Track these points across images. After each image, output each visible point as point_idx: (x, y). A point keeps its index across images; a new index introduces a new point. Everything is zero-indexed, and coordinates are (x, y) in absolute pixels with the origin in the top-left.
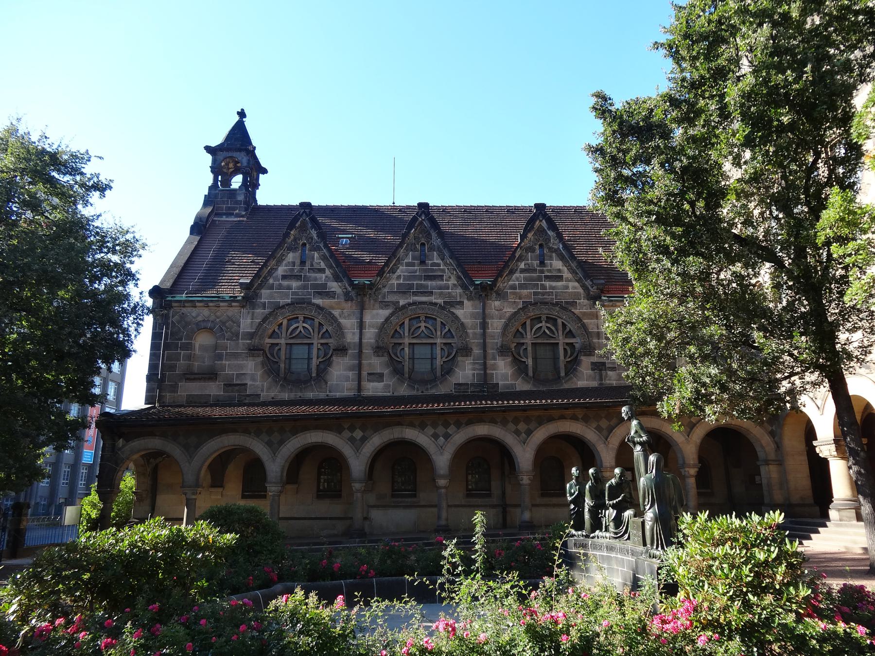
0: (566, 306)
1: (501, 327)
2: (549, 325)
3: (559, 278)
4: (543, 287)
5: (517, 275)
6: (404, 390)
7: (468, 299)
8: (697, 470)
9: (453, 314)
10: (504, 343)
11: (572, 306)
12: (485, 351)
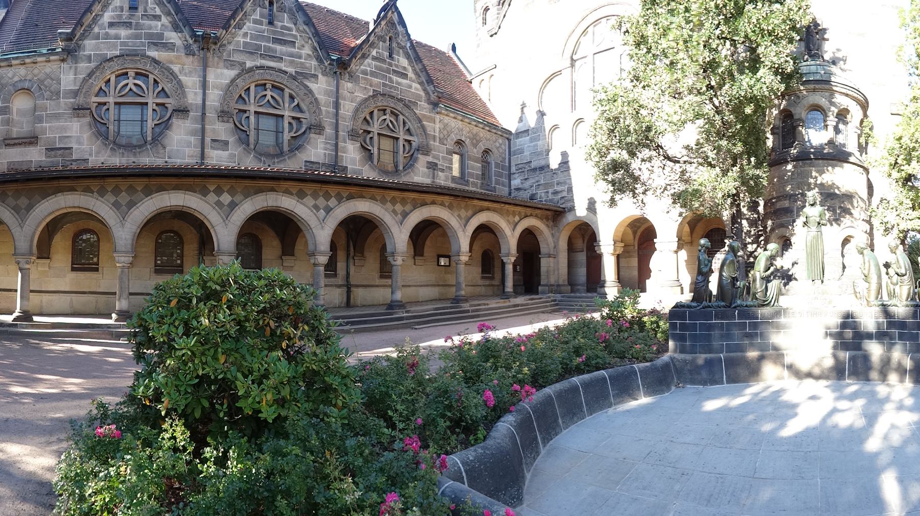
0: (409, 105)
1: (352, 110)
2: (392, 119)
3: (404, 76)
4: (391, 80)
5: (368, 61)
6: (250, 163)
7: (323, 75)
8: (515, 258)
9: (306, 87)
10: (355, 127)
11: (414, 105)
12: (337, 131)
